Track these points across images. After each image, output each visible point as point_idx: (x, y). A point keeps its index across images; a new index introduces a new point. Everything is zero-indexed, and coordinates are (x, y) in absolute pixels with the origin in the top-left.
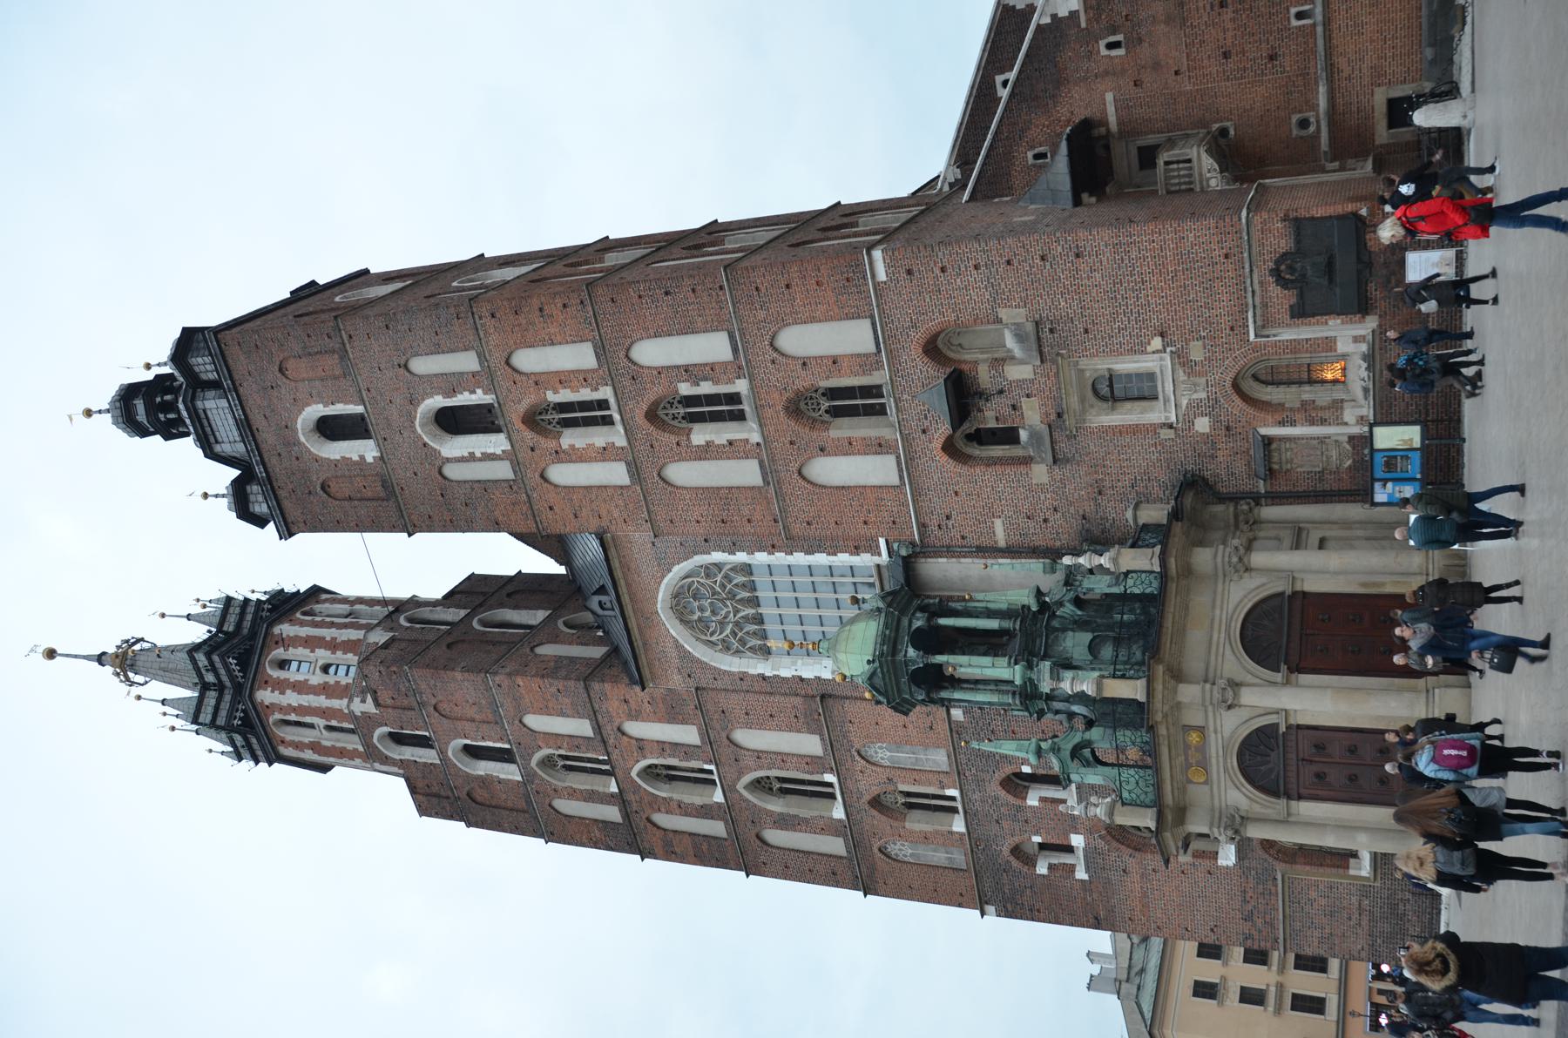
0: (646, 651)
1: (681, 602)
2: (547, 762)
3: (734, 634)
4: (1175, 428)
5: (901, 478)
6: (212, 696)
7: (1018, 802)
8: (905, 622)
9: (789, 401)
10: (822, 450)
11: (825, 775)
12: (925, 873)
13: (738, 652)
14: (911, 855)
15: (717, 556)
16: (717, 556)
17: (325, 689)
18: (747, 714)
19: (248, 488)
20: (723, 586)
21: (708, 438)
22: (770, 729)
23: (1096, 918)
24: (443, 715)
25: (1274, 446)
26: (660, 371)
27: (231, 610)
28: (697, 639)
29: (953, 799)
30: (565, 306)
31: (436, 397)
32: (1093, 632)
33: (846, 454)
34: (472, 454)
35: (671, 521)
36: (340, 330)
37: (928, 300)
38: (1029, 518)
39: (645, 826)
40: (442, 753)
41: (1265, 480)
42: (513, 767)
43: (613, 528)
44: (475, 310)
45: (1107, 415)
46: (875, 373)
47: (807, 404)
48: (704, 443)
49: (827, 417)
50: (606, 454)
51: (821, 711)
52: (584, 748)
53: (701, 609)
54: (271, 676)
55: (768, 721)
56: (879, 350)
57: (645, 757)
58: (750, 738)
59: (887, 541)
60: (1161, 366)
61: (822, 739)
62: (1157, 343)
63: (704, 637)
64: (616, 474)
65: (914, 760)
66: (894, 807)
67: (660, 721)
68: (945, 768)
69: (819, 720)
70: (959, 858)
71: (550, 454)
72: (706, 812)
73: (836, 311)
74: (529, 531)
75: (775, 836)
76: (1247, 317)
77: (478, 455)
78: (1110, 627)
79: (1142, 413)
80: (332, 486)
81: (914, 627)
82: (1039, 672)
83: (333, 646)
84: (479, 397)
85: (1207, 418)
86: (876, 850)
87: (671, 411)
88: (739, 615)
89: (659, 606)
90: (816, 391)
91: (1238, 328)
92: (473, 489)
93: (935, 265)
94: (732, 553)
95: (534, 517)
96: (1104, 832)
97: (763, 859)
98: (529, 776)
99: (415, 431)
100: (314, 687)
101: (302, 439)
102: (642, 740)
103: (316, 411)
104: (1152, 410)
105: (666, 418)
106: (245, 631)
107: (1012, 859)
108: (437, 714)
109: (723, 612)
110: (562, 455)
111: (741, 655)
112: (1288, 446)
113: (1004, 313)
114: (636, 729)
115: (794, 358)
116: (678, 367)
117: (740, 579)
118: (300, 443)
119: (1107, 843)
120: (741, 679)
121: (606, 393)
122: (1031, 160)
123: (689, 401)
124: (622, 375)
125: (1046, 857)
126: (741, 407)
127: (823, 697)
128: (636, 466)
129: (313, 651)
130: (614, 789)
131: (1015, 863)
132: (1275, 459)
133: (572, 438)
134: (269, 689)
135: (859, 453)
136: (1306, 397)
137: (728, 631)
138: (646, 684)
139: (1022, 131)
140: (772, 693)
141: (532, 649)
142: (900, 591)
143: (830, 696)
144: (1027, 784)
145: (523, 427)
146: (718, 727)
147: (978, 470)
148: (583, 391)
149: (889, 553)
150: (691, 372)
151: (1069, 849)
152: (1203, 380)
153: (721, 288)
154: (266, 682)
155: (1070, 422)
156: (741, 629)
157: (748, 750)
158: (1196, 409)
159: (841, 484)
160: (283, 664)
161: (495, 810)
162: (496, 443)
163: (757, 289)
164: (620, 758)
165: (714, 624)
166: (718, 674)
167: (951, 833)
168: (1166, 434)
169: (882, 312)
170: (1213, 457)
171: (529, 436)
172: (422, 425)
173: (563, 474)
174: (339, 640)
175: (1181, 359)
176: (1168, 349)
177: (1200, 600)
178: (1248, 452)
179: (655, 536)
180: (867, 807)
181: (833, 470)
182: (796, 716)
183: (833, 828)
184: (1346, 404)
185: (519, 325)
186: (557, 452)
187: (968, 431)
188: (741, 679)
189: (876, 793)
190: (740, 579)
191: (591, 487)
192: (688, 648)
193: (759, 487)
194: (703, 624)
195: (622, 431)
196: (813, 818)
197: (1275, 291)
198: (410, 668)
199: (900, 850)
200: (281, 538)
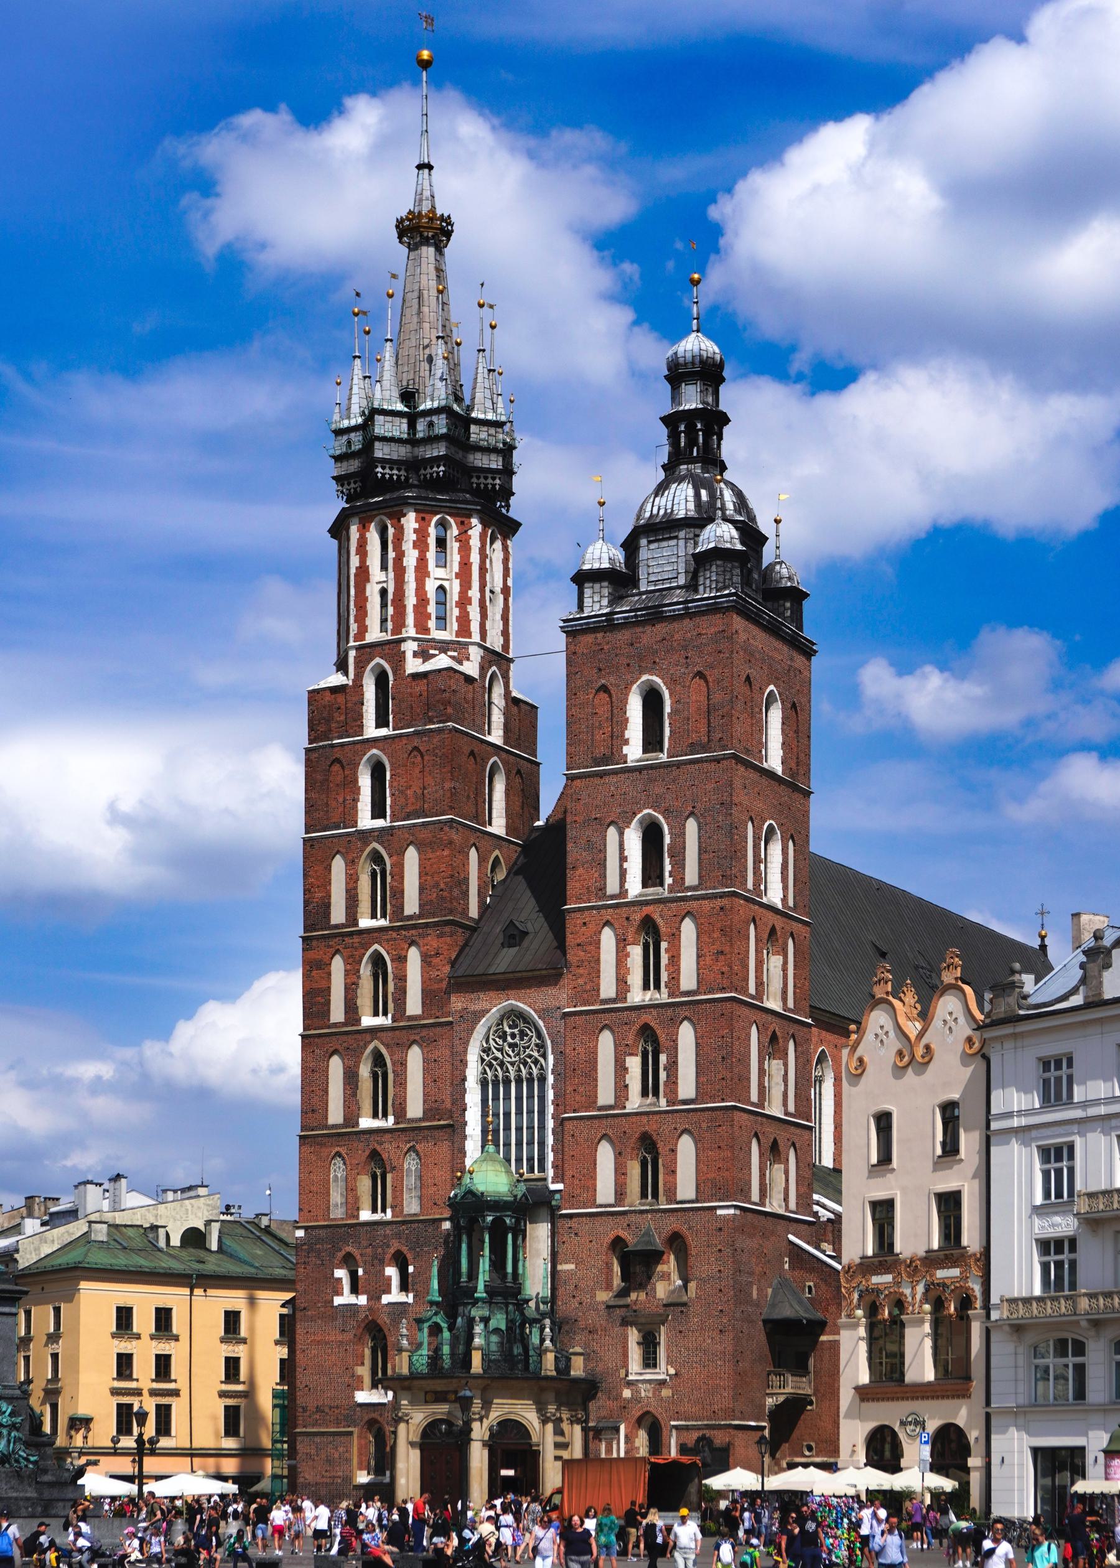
1: (515, 1016)
2: (377, 858)
3: (496, 1059)
5: (601, 1206)
10: (620, 1154)
13: (483, 1060)
14: (336, 1176)
15: (551, 1058)
16: (551, 1058)
17: (422, 601)
19: (605, 584)
20: (530, 1056)
23: (305, 1309)
24: (410, 754)
26: (675, 1041)
27: (492, 431)
28: (490, 1029)
29: (384, 1210)
30: (723, 973)
39: (331, 947)
40: (374, 741)
51: (442, 1123)
52: (394, 903)
53: (513, 1036)
54: (429, 525)
56: (678, 1203)
57: (392, 961)
58: (415, 1057)
59: (561, 1191)
61: (420, 1120)
62: (672, 1371)
67: (423, 982)
68: (406, 1211)
70: (337, 1213)
71: (623, 934)
72: (352, 1009)
74: (568, 897)
75: (336, 1066)
77: (625, 865)
81: (506, 1219)
82: (483, 1308)
83: (464, 602)
84: (668, 880)
86: (337, 1149)
89: (513, 1002)
91: (678, 1416)
96: (370, 1318)
97: (317, 1051)
101: (645, 677)
107: (343, 1253)
109: (511, 1053)
114: (414, 956)
116: (676, 1057)
117: (535, 1071)
118: (641, 673)
119: (363, 1320)
120: (461, 1061)
122: (808, 1284)
124: (674, 1011)
126: (650, 1095)
127: (451, 1126)
129: (457, 576)
131: (340, 1255)
133: (636, 953)
134: (417, 526)
139: (826, 1281)
141: (474, 844)
143: (454, 1131)
145: (643, 915)
150: (673, 1066)
152: (650, 1395)
153: (723, 1100)
154: (423, 519)
160: (443, 525)
162: (635, 887)
163: (720, 1126)
166: (466, 1043)
167: (358, 1209)
168: (622, 1373)
171: (637, 917)
172: (649, 814)
173: (608, 938)
174: (469, 608)
175: (662, 1383)
181: (605, 1155)
183: (351, 1118)
186: (625, 940)
188: (461, 1061)
192: (481, 1023)
193: (596, 1102)
196: (357, 1103)
197: (695, 1435)
199: (339, 1168)
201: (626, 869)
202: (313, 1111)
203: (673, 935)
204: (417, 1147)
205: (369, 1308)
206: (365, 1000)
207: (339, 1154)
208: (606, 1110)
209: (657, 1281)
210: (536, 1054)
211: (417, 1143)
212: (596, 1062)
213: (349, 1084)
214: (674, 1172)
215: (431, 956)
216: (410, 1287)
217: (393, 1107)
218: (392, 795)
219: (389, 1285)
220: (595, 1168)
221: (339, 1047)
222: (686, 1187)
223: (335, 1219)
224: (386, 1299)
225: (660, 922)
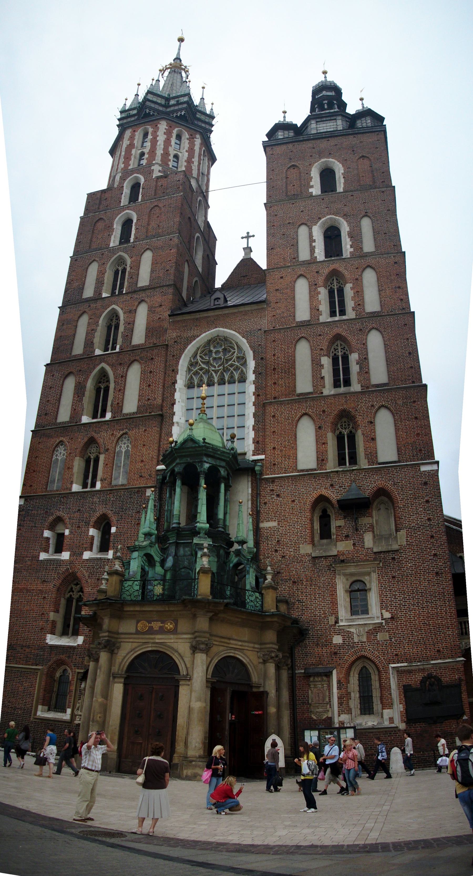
3: (201, 369)
4: (335, 625)
5: (302, 471)
6: (163, 102)
7: (91, 523)
8: (223, 464)
9: (349, 412)
10: (320, 428)
11: (110, 413)
12: (46, 466)
14: (57, 459)
16: (251, 364)
18: (151, 372)
20: (232, 365)
22: (140, 384)
24: (151, 210)
25: (325, 678)
28: (198, 349)
29: (93, 485)
30: (402, 300)
31: (348, 227)
32: (217, 573)
33: (317, 441)
34: (314, 241)
35: (274, 341)
36: (387, 187)
37: (410, 492)
38: (278, 541)
41: (304, 673)
42: (117, 243)
44: (399, 254)
45: (343, 587)
46: (366, 461)
47: (345, 422)
48: (322, 363)
49: (337, 432)
50: (315, 310)
51: (152, 414)
56: (380, 464)
57: (124, 313)
59: (263, 460)
60: (374, 618)
61: (134, 413)
62: (387, 615)
63: (199, 352)
65: (119, 465)
66: (88, 451)
67: (148, 324)
68: (114, 483)
69: (146, 412)
71: (314, 281)
76: (404, 663)
77: (314, 244)
79: (344, 607)
80: (294, 170)
81: (220, 469)
85: (342, 642)
86: (61, 439)
87: (339, 348)
89: (221, 329)
90: (353, 428)
92: (293, 239)
93: (430, 497)
94: (254, 372)
99: (328, 214)
100: (168, 148)
102: (136, 313)
103: (339, 170)
104: (346, 612)
105: (336, 344)
106: (196, 122)
107: (54, 516)
108: (152, 206)
109: (215, 364)
110: (314, 287)
111: (188, 372)
112: (326, 685)
113: (403, 533)
115: (374, 417)
116: (367, 354)
117: (236, 376)
120: (173, 371)
123: (346, 359)
125: (53, 536)
126: (342, 386)
127: (162, 416)
128: (308, 325)
130: (104, 295)
131: (51, 518)
132: (316, 679)
133: (323, 293)
135: (317, 449)
136: (352, 695)
137: (203, 366)
138: (172, 317)
140: (164, 387)
143: (162, 420)
144: (101, 529)
147: (308, 514)
149: (255, 460)
151: (59, 550)
152: (365, 639)
155: (338, 567)
156: (204, 373)
157: (127, 371)
158: (347, 635)
159: (298, 436)
160: (179, 137)
161: (91, 232)
163: (414, 402)
164: (124, 300)
165: (207, 358)
167: (72, 483)
168: (332, 620)
170: (317, 645)
171: (326, 271)
175: (378, 628)
176: (383, 621)
178: (320, 664)
179: (265, 331)
180: (89, 436)
182: (149, 399)
184: (350, 715)
185: (390, 275)
186: (316, 285)
187: (328, 510)
189: (99, 441)
190: (236, 376)
193: (295, 391)
194: (207, 352)
195: (328, 320)
196: (82, 405)
198: (181, 195)
199: (60, 453)
200: (263, 142)
201: (315, 246)
202: (46, 414)
203: (357, 279)
204: (130, 433)
205: (70, 562)
206: (99, 338)
207: (61, 443)
210: (236, 363)
212: (294, 362)
213: (77, 394)
214: (374, 439)
215: (155, 307)
216: (111, 544)
217: (112, 406)
218: (137, 229)
219: (92, 544)
220: (296, 440)
221: (74, 371)
223: (51, 491)
224: (87, 555)
225: (346, 273)
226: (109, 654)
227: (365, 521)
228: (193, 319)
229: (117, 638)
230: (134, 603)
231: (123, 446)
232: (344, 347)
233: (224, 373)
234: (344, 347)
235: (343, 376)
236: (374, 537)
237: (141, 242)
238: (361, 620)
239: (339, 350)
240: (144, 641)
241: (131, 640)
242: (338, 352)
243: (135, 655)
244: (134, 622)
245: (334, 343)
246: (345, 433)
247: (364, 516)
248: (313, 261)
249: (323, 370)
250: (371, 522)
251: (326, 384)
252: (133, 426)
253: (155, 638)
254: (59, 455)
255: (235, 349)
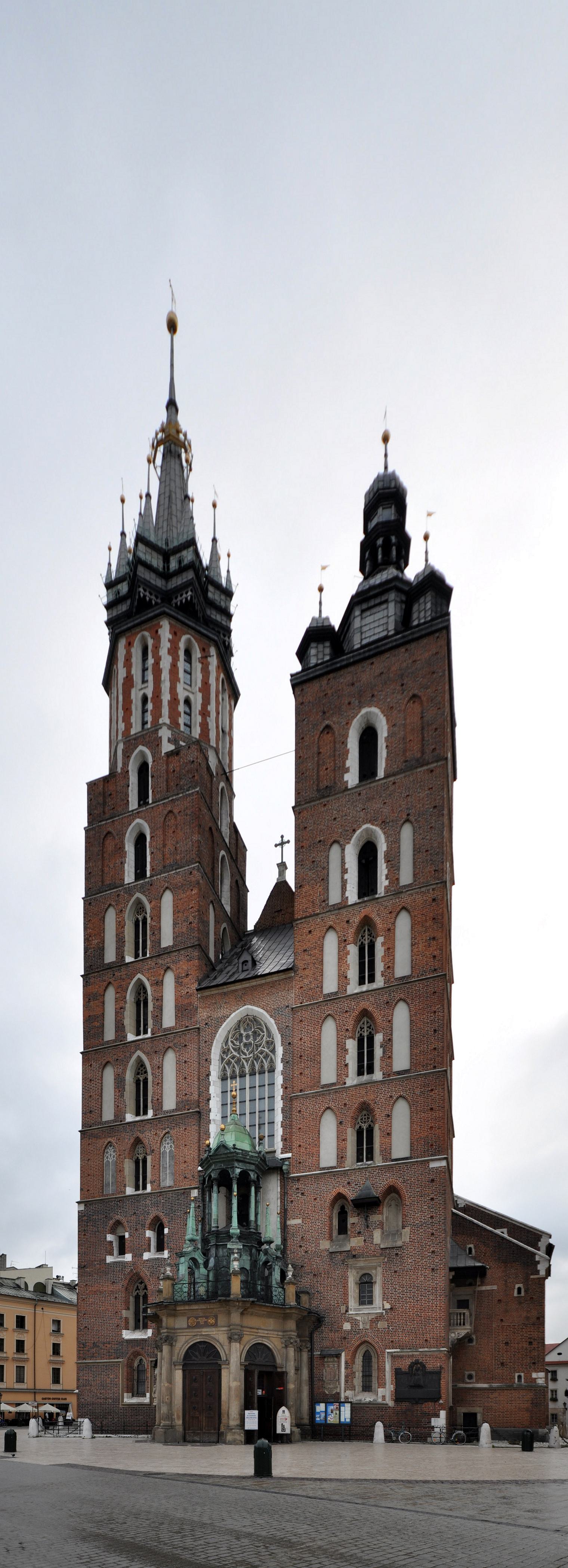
0: (221, 994)
4: (345, 1313)
9: (369, 1105)
11: (152, 1110)
21: (350, 1051)
35: (301, 1021)
41: (320, 1354)
43: (297, 978)
45: (354, 1280)
48: (347, 1048)
50: (343, 978)
55: (182, 1077)
61: (173, 1111)
64: (330, 985)
66: (136, 1152)
73: (416, 1137)
74: (296, 912)
78: (253, 1278)
88: (245, 1063)
95: (305, 918)
98: (130, 890)
105: (362, 1022)
120: (206, 1060)
121: (379, 982)
123: (371, 1039)
126: (365, 1073)
127: (199, 1112)
138: (199, 992)
142: (266, 1164)
143: (200, 1117)
146: (176, 1041)
148: (382, 964)
158: (355, 1323)
169: (413, 1163)
170: (331, 1331)
173: (331, 942)
177: (271, 1323)
179: (292, 1009)
181: (329, 1128)
182: (186, 1094)
189: (144, 1142)
191: (322, 964)
208: (328, 1087)
209: (374, 1229)
211: (171, 1129)
222: (401, 1147)
226: (169, 1347)
227: (375, 1218)
228: (221, 994)
229: (174, 1333)
230: (183, 1303)
231: (167, 1146)
232: (371, 1025)
233: (255, 1062)
234: (371, 1025)
235: (367, 1061)
236: (383, 1233)
237: (159, 877)
238: (366, 1310)
239: (365, 1029)
240: (195, 1334)
241: (184, 1334)
242: (364, 1032)
243: (189, 1346)
244: (185, 1319)
245: (360, 1021)
246: (365, 1128)
247: (375, 1213)
248: (343, 905)
249: (347, 1056)
250: (381, 1219)
251: (349, 1073)
252: (174, 1125)
253: (201, 1331)
254: (109, 1157)
255: (263, 1032)
